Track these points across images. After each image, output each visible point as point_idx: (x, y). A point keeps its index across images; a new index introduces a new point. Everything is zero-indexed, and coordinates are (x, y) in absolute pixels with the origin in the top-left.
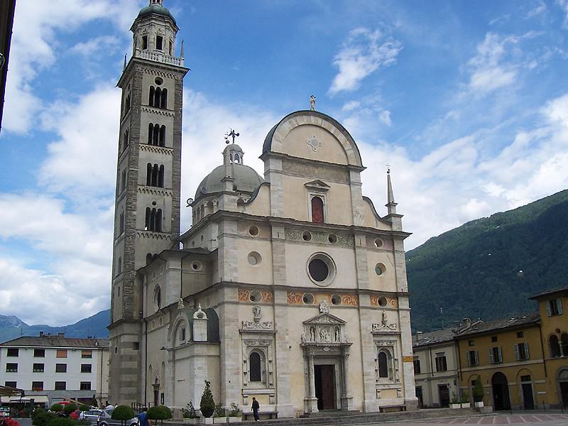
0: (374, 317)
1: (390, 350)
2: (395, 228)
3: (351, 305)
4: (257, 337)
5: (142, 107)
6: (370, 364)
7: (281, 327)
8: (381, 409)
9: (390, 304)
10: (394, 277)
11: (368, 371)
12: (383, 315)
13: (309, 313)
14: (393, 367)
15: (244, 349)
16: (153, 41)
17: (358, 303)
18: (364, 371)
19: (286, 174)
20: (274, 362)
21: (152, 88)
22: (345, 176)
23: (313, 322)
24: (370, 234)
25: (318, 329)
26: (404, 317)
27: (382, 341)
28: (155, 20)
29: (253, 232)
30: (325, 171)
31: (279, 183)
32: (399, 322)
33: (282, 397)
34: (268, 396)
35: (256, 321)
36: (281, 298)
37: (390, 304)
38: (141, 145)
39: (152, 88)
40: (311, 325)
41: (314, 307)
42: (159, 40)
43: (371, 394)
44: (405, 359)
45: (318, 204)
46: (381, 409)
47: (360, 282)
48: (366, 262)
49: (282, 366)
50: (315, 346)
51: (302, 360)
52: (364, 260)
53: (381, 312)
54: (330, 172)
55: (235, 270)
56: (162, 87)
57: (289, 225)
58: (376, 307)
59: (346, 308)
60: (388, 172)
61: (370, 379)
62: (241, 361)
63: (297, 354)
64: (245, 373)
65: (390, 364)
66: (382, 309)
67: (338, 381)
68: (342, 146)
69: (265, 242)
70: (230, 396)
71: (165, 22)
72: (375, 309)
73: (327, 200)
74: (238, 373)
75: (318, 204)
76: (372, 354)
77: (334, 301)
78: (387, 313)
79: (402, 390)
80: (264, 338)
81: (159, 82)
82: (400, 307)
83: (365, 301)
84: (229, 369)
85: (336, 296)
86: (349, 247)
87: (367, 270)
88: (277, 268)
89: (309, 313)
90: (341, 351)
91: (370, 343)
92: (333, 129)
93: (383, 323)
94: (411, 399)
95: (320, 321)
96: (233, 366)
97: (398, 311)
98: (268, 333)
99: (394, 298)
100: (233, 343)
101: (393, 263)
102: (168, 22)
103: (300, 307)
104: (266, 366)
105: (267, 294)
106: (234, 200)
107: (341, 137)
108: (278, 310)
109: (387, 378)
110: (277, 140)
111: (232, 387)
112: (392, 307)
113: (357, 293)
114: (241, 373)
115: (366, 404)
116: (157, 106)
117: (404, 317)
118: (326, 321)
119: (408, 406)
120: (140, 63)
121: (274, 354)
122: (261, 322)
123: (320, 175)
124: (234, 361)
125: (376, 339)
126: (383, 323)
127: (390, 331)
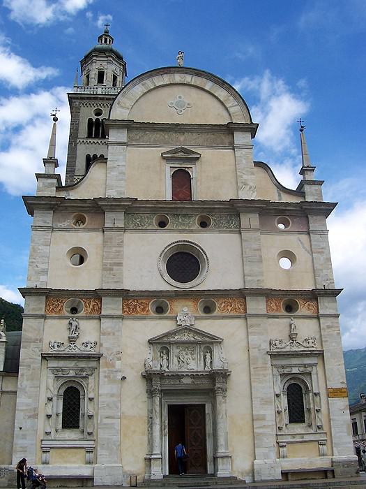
0: (276, 330)
2: (309, 199)
3: (232, 314)
4: (71, 364)
5: (78, 140)
6: (265, 402)
7: (108, 349)
9: (303, 309)
10: (310, 269)
11: (262, 412)
12: (291, 325)
13: (160, 327)
14: (312, 406)
15: (51, 381)
16: (93, 76)
17: (245, 310)
19: (133, 146)
20: (95, 400)
21: (90, 120)
22: (227, 140)
23: (165, 340)
24: (267, 211)
25: (174, 351)
26: (328, 327)
27: (290, 366)
28: (96, 56)
29: (80, 220)
30: (195, 135)
31: (121, 157)
33: (104, 452)
35: (72, 340)
36: (111, 307)
37: (303, 309)
38: (76, 178)
39: (90, 120)
40: (161, 344)
41: (167, 318)
42: (101, 76)
43: (266, 450)
44: (334, 393)
45: (182, 180)
46: (285, 474)
48: (260, 250)
49: (108, 405)
50: (161, 375)
51: (145, 397)
52: (255, 246)
53: (286, 321)
54: (202, 138)
55: (45, 272)
56: (100, 118)
57: (131, 208)
58: (278, 314)
59: (224, 317)
60: (301, 130)
61: (264, 426)
62: (43, 399)
63: (136, 388)
64: (49, 416)
65: (309, 402)
66: (289, 317)
67: (209, 429)
68: (222, 103)
69: (93, 234)
70: (18, 449)
71: (107, 57)
72: (277, 317)
73: (195, 170)
74: (36, 416)
75: (182, 180)
76: (271, 387)
77: (208, 310)
78: (296, 322)
79: (329, 441)
80: (82, 364)
81: (98, 113)
82: (321, 312)
83: (257, 306)
84: (21, 410)
85: (209, 302)
86: (231, 232)
87: (262, 262)
88: (112, 266)
89: (160, 327)
90: (215, 381)
91: (265, 368)
92: (209, 85)
93: (292, 337)
94: (344, 457)
95: (177, 338)
96: (27, 405)
97: (318, 318)
98: (88, 358)
99: (311, 299)
100: (30, 372)
101: (309, 249)
102: (110, 56)
103: (144, 318)
104: (86, 408)
105: (93, 303)
106: (53, 184)
107: (222, 93)
108: (106, 324)
109: (304, 425)
110: (123, 107)
111: (24, 437)
113: (242, 295)
114: (42, 417)
115: (255, 467)
116: (97, 136)
117: (328, 327)
118: (186, 337)
119: (338, 470)
120: (77, 98)
121: (96, 387)
122: (78, 342)
123: (184, 140)
125: (275, 362)
126: (292, 337)
127: (302, 349)
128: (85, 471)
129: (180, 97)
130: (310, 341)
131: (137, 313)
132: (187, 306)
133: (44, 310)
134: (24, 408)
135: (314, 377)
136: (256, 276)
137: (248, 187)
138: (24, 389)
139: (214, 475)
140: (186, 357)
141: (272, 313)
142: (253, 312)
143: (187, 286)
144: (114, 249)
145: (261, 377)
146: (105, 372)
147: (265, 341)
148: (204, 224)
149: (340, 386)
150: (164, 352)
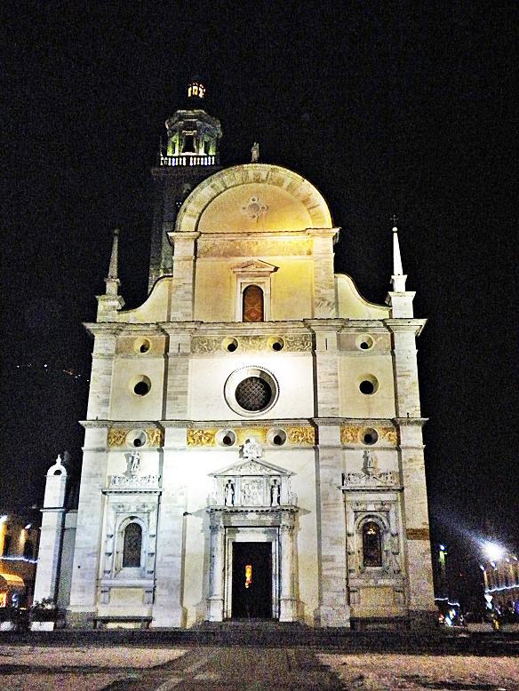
1: (382, 515)
8: (353, 621)
9: (382, 441)
11: (331, 553)
18: (323, 554)
23: (230, 473)
32: (401, 472)
34: (141, 590)
36: (175, 437)
44: (413, 534)
47: (320, 406)
49: (169, 543)
58: (354, 445)
67: (275, 570)
112: (389, 444)
124: (89, 535)
128: (144, 613)
129: (254, 200)
130: (389, 476)
131: (203, 444)
132: (255, 437)
133: (105, 442)
134: (84, 546)
135: (392, 516)
136: (331, 403)
137: (327, 303)
138: (83, 526)
139: (278, 619)
140: (252, 491)
141: (347, 444)
142: (326, 444)
143: (258, 415)
144: (178, 377)
145: (332, 514)
146: (167, 507)
147: (337, 475)
148: (277, 347)
149: (420, 527)
150: (230, 486)
